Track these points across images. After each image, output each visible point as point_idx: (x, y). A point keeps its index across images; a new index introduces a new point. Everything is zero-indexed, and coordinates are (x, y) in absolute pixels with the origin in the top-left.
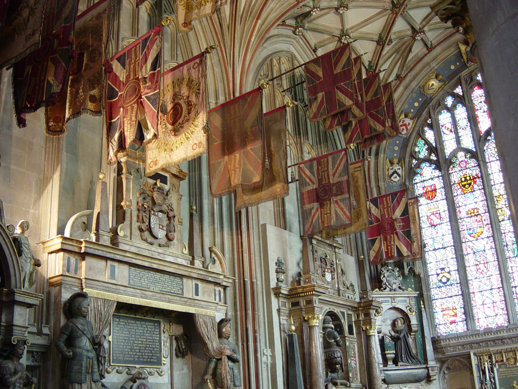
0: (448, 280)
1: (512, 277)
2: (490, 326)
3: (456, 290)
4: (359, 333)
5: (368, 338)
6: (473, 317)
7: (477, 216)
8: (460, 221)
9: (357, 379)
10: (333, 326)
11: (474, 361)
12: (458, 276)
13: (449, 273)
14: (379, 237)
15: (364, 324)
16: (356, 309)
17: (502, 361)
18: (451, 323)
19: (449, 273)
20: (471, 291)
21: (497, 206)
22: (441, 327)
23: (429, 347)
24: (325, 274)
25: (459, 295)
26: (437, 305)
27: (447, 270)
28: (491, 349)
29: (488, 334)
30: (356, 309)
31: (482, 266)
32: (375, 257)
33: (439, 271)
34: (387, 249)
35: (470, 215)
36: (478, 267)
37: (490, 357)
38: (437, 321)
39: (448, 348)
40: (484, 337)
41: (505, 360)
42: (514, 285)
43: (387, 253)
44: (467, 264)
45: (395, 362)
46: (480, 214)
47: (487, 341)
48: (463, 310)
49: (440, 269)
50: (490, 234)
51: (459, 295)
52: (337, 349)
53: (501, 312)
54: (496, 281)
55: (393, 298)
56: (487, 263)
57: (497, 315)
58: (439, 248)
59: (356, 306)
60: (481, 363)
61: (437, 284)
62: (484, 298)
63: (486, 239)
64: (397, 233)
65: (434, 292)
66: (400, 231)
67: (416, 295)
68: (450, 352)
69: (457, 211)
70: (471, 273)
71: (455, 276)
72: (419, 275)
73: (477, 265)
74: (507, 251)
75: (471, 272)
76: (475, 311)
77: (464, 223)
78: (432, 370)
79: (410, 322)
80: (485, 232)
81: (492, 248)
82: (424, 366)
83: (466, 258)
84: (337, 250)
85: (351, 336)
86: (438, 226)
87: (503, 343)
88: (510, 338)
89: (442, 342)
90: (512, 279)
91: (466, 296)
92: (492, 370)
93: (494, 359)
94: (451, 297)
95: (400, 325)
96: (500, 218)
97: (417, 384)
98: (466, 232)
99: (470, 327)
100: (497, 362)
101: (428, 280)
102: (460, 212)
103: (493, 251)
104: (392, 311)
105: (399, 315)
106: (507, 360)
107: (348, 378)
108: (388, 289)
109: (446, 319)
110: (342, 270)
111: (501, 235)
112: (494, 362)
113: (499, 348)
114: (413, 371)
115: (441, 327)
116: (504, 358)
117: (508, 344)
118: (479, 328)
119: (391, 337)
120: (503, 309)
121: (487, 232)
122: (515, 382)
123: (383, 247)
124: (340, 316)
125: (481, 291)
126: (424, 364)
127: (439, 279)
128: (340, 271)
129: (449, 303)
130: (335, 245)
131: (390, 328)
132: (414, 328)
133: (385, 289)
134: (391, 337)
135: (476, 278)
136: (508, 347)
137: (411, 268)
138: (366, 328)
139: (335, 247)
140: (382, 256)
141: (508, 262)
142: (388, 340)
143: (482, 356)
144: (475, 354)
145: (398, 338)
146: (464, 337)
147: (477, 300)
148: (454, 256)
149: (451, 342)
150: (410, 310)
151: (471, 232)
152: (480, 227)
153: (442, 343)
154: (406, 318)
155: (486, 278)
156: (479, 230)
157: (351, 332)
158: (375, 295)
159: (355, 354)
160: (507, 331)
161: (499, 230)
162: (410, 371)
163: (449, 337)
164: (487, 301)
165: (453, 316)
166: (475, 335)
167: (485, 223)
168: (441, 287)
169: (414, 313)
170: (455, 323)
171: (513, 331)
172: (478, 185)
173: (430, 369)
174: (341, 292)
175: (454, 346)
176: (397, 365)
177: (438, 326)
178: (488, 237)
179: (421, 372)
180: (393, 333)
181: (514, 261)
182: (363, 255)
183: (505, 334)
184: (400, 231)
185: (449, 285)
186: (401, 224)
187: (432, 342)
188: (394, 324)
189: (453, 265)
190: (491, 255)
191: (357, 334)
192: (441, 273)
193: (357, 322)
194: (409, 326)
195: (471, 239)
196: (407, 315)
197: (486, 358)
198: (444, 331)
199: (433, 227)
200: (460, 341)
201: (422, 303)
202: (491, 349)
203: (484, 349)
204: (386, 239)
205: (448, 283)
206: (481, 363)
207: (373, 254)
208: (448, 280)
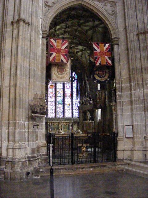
11: (48, 123)
54: (54, 108)
88: (56, 120)
121: (54, 98)
172: (54, 88)
190: (54, 103)
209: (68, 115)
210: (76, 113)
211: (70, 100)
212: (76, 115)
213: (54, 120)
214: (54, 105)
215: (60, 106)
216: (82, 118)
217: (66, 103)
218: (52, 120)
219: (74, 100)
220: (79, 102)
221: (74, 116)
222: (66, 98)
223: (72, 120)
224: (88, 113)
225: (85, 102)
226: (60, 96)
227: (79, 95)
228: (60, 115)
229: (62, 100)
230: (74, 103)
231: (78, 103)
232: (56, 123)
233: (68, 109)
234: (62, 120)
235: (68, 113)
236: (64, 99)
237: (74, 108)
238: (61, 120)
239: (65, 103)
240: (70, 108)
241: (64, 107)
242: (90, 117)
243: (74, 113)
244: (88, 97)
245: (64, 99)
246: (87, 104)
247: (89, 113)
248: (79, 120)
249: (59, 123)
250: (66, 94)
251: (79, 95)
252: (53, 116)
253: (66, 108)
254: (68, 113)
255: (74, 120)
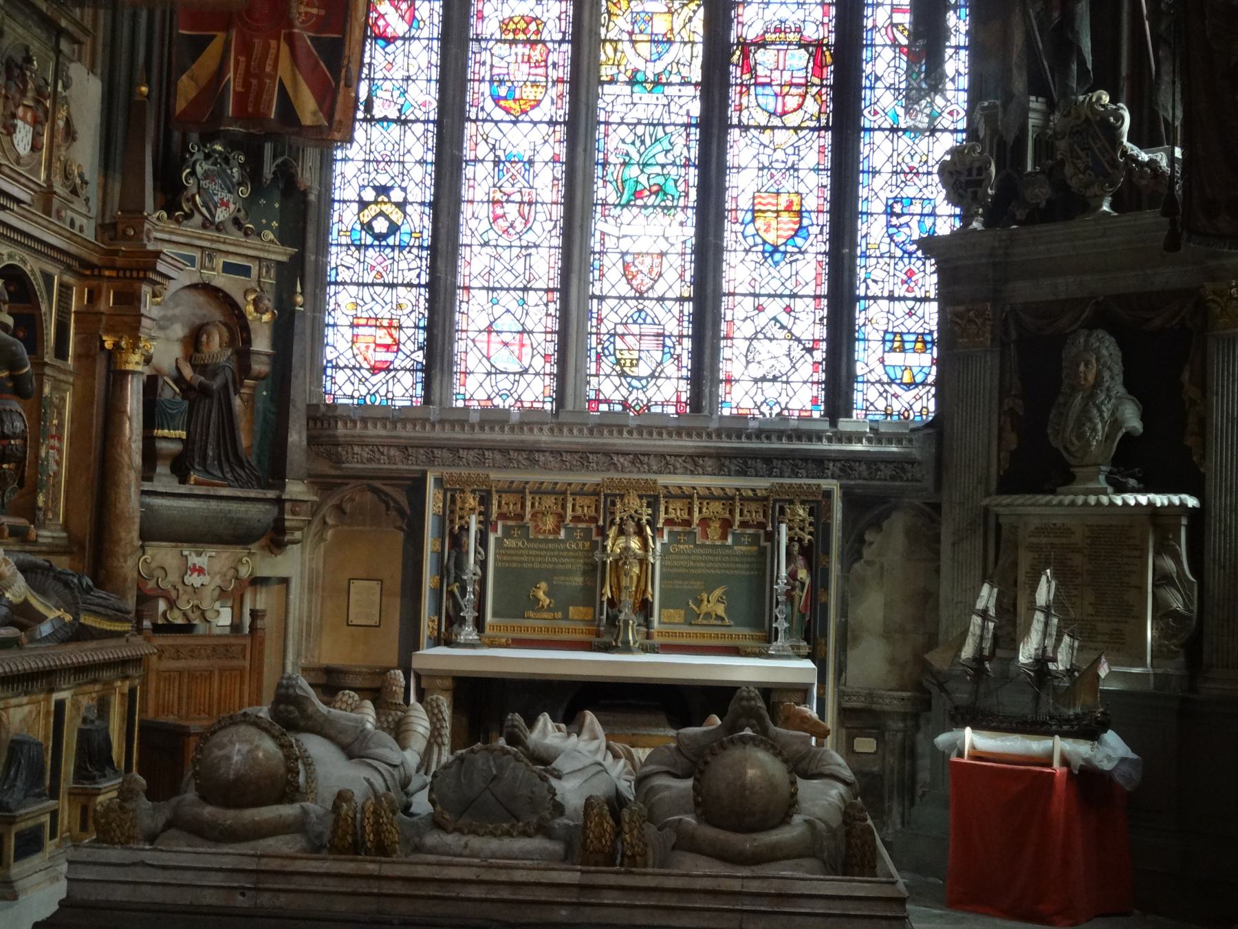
0: (394, 228)
1: (597, 264)
2: (498, 401)
3: (412, 267)
4: (85, 356)
5: (117, 378)
6: (451, 363)
7: (533, 43)
8: (474, 46)
9: (56, 515)
10: (10, 321)
12: (427, 222)
13: (402, 206)
14: (220, 37)
15: (110, 330)
16: (83, 268)
17: (521, 517)
18: (374, 370)
19: (402, 206)
20: (460, 281)
21: (603, 31)
22: (341, 376)
23: (297, 437)
24: (15, 126)
25: (419, 286)
26: (342, 304)
27: (397, 195)
28: (493, 476)
29: (492, 429)
30: (83, 268)
31: (512, 210)
32: (194, 103)
33: (369, 195)
34: (246, 84)
35: (511, 36)
36: (499, 211)
37: (485, 500)
38: (330, 354)
39: (356, 449)
40: (479, 435)
41: (528, 516)
42: (597, 293)
43: (241, 99)
44: (466, 194)
45: (180, 469)
46: (544, 42)
47: (482, 449)
48: (422, 336)
49: (375, 188)
50: (561, 113)
51: (419, 286)
52: (15, 405)
53: (538, 363)
54: (545, 266)
55: (210, 253)
56: (530, 203)
57: (526, 371)
58: (385, 119)
59: (95, 258)
60: (452, 512)
61: (356, 236)
62: (498, 310)
63: (544, 128)
64: (291, 40)
65: (340, 260)
66: (305, 36)
67: (284, 259)
68: (358, 460)
69: (473, 10)
70: (473, 224)
71: (418, 221)
72: (305, 194)
73: (495, 202)
74: (600, 182)
75: (474, 220)
76: (459, 346)
77: (485, 56)
78: (293, 513)
79: (248, 341)
80: (546, 103)
81: (555, 159)
82: (271, 494)
83: (469, 171)
84: (64, 46)
85: (59, 363)
86: (399, 43)
87: (533, 462)
88: (557, 453)
89: (340, 424)
90: (597, 273)
91: (441, 291)
92: (483, 542)
93: (495, 508)
94: (392, 286)
95: (215, 344)
96: (606, 72)
97: (239, 551)
98: (485, 87)
99: (436, 396)
100: (502, 516)
101: (329, 216)
102: (481, 18)
103: (559, 170)
104: (201, 299)
105: (216, 314)
106: (534, 515)
107: (30, 512)
108: (197, 219)
109: (361, 351)
110: (68, 122)
111: (594, 129)
112: (494, 517)
113: (518, 477)
114: (234, 506)
115: (341, 376)
116: (528, 509)
117: (546, 468)
118: (460, 404)
119: (179, 379)
120: (546, 357)
121: (552, 104)
122: (543, 585)
123: (231, 75)
124: (38, 284)
125: (494, 289)
126: (269, 487)
127: (366, 220)
128: (61, 124)
129: (381, 304)
130: (64, 23)
131: (177, 351)
132: (260, 366)
133: (188, 216)
134: (179, 379)
135: (486, 244)
136: (548, 478)
137: (284, 163)
138: (116, 345)
139: (60, 32)
140: (221, 104)
141: (598, 216)
142: (169, 391)
143: (463, 491)
144: (439, 482)
145: (204, 391)
146: (414, 422)
147: (473, 313)
148: (430, 157)
149: (371, 431)
150: (256, 303)
151: (503, 91)
152: (535, 84)
153: (341, 430)
154: (239, 328)
155: (515, 251)
156: (530, 93)
157: (61, 352)
158: (160, 232)
159: (60, 426)
160: (551, 430)
161: (592, 109)
162: (224, 505)
163: (367, 414)
164: (506, 323)
165: (387, 347)
166: (453, 423)
167: (553, 74)
168: (367, 247)
169: (266, 317)
170: (388, 370)
171: (571, 431)
173: (288, 506)
174: (56, 202)
175: (376, 447)
176: (183, 480)
177: (329, 371)
178: (552, 123)
179: (258, 514)
180: (188, 372)
181: (616, 218)
182: (148, 83)
183: (544, 437)
184: (305, 36)
185: (393, 248)
186: (314, 11)
187: (309, 419)
188: (194, 341)
189: (418, 185)
190: (547, 184)
191: (78, 357)
192: (376, 202)
193: (88, 317)
194: (244, 354)
195: (498, 114)
196: (242, 316)
197: (472, 502)
198: (348, 389)
199: (381, 42)
200: (400, 432)
201: (299, 289)
202: (493, 476)
203: (474, 472)
204: (246, 48)
205: (391, 241)
206: (452, 512)
207: (187, 89)
208: (394, 228)
209: (770, 377)
210: (895, 359)
211: (815, 152)
212: (898, 381)
213: (531, 453)
214: (545, 229)
215: (646, 241)
216: (982, 445)
217: (742, 186)
218: (504, 450)
219: (877, 151)
220: (959, 177)
221: (871, 401)
222: (749, 106)
223: (819, 463)
224: (1101, 358)
225: (1052, 173)
226: (651, 71)
227: (956, 64)
228: (643, 375)
229: (686, 146)
230: (874, 193)
231: (938, 193)
232: (560, 494)
233: (773, 278)
234: (666, 461)
235: (772, 355)
236: (713, 127)
237: (875, 274)
238: (637, 458)
239: (732, 179)
240: (809, 270)
241: (708, 253)
242: (1132, 419)
243: (868, 358)
244: (1106, 78)
245: (713, 127)
246: (1087, 206)
247: (1108, 348)
248: (940, 464)
249: (606, 498)
250: (745, 46)
251: (956, 64)
252: (536, 392)
253: (738, 270)
254: (772, 355)
255: (848, 463)
